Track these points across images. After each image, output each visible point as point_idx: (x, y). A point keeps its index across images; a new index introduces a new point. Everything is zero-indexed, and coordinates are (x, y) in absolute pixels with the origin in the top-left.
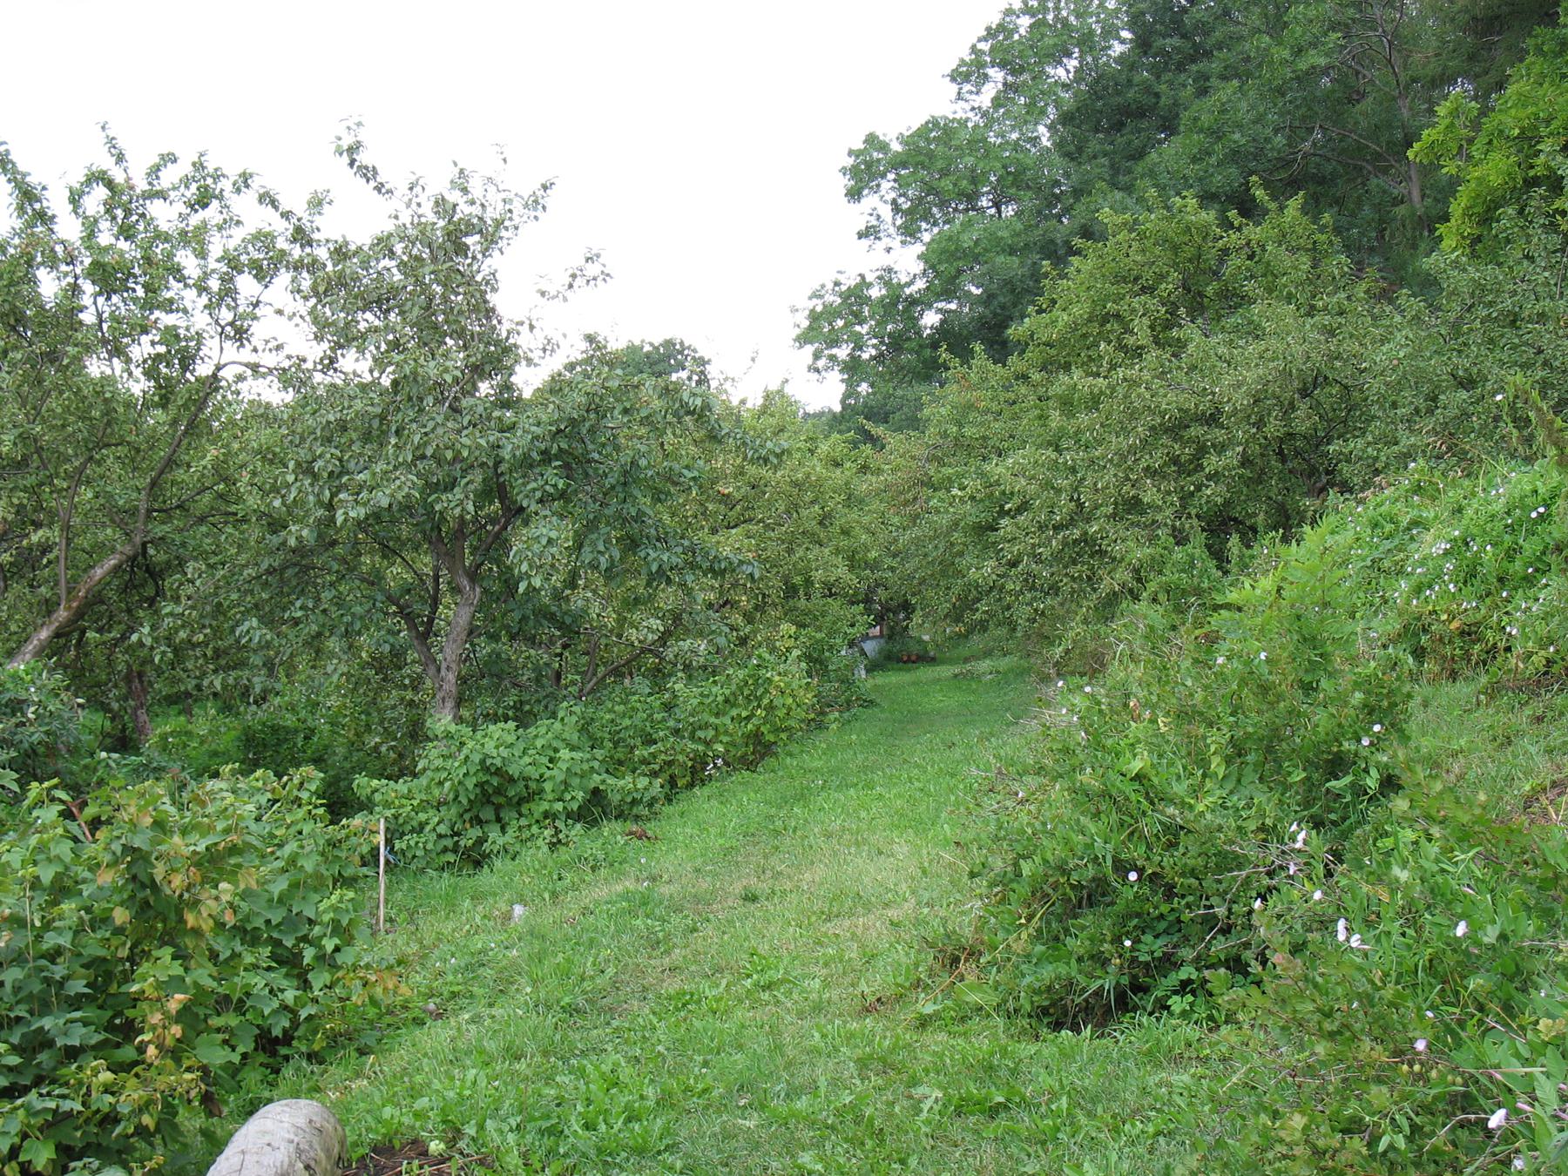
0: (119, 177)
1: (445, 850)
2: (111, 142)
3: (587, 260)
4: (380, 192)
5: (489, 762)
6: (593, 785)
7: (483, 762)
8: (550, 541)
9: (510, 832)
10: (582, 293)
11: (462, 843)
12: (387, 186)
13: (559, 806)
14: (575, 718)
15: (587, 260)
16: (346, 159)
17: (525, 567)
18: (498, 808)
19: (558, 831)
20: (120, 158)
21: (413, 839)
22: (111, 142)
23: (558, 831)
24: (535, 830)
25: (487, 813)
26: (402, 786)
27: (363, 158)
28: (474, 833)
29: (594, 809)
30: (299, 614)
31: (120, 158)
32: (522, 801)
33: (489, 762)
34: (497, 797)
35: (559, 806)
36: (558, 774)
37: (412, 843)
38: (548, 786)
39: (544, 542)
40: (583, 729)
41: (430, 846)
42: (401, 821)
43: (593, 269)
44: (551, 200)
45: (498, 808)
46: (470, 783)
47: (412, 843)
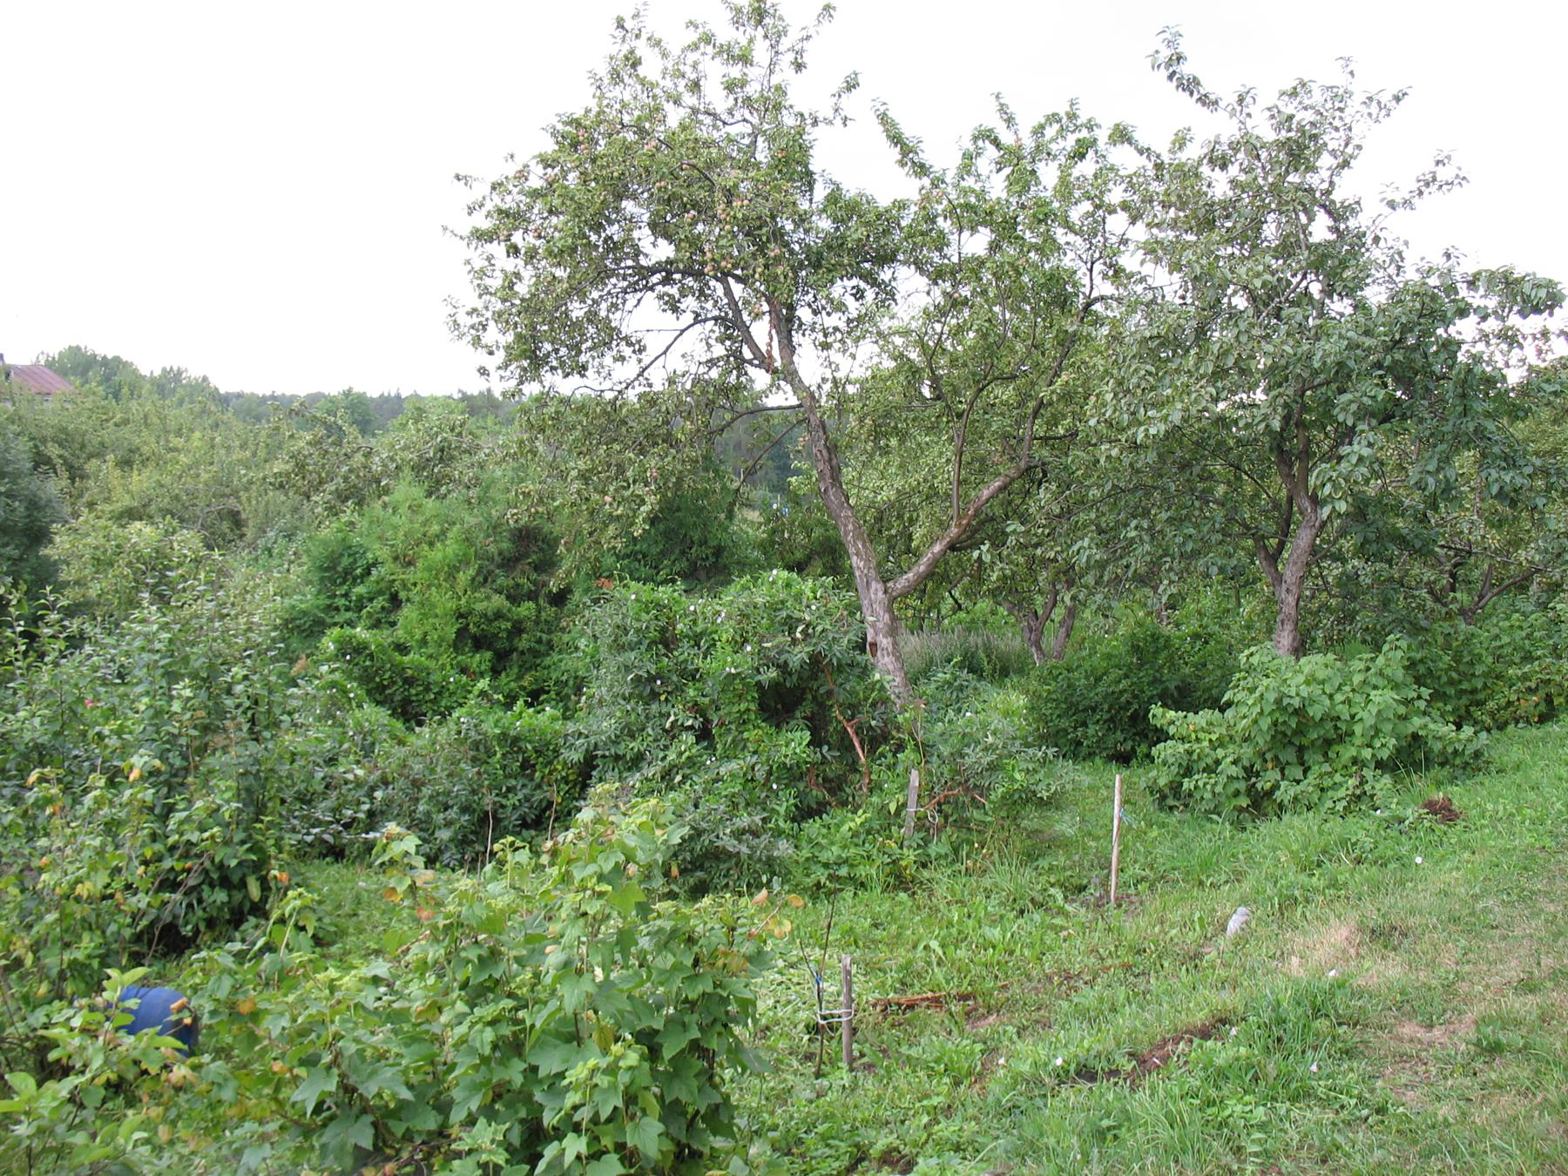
0: (1007, 138)
1: (1237, 794)
2: (1003, 109)
3: (1438, 163)
4: (1204, 104)
5: (1285, 701)
6: (1411, 730)
7: (1278, 701)
8: (1361, 459)
9: (1311, 778)
10: (1433, 198)
11: (1259, 786)
12: (1213, 97)
13: (1367, 754)
14: (1400, 653)
15: (1438, 163)
16: (1164, 73)
17: (1328, 489)
18: (1301, 750)
19: (1363, 782)
20: (1010, 121)
21: (1202, 778)
22: (1003, 109)
23: (1363, 782)
24: (1338, 778)
25: (1289, 755)
26: (1204, 717)
27: (1186, 69)
28: (1272, 775)
29: (1410, 757)
30: (1133, 534)
31: (1010, 121)
32: (1328, 743)
33: (1285, 701)
34: (1300, 738)
35: (1367, 754)
36: (1368, 716)
37: (1200, 784)
38: (1358, 729)
39: (1354, 460)
40: (1411, 665)
41: (1219, 789)
42: (1195, 757)
43: (1444, 174)
44: (1399, 111)
45: (1301, 750)
46: (1265, 723)
47: (1200, 784)
